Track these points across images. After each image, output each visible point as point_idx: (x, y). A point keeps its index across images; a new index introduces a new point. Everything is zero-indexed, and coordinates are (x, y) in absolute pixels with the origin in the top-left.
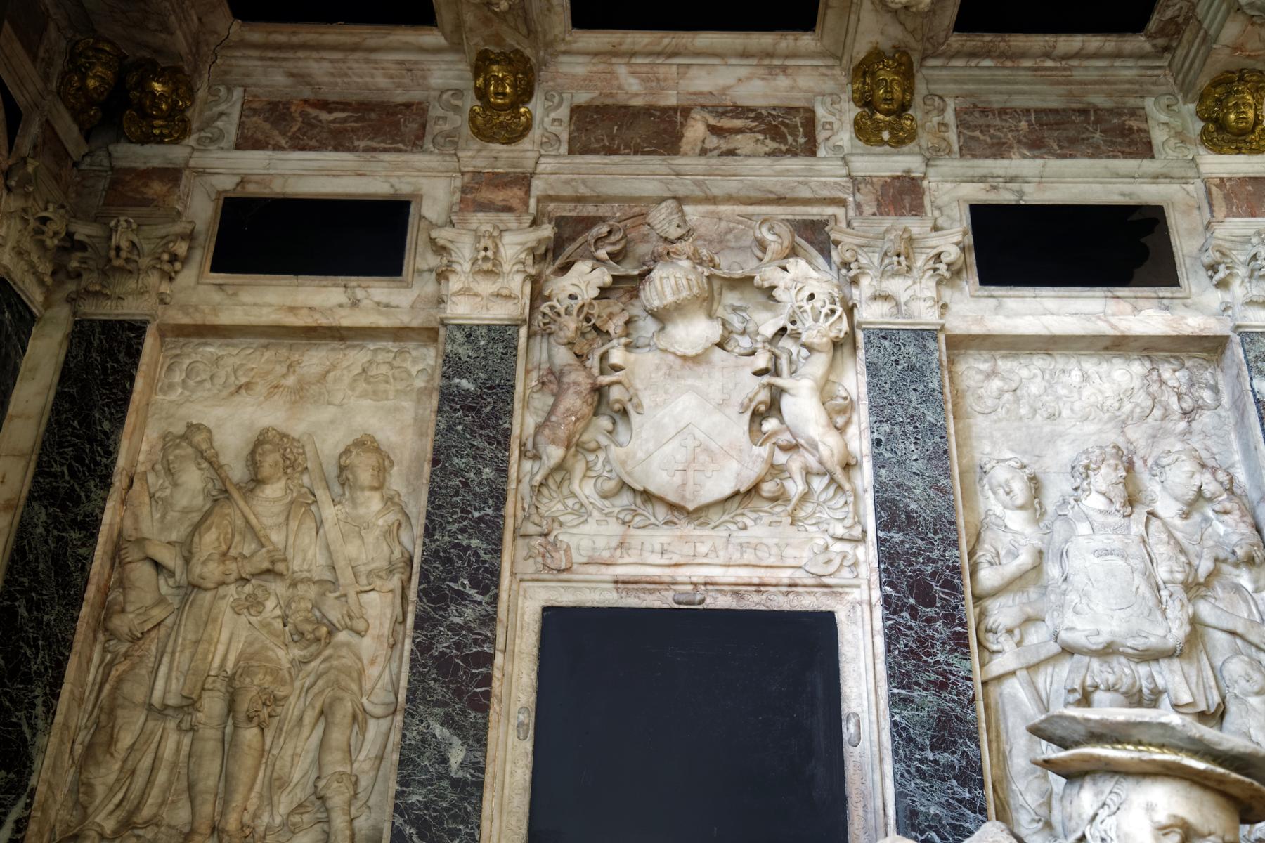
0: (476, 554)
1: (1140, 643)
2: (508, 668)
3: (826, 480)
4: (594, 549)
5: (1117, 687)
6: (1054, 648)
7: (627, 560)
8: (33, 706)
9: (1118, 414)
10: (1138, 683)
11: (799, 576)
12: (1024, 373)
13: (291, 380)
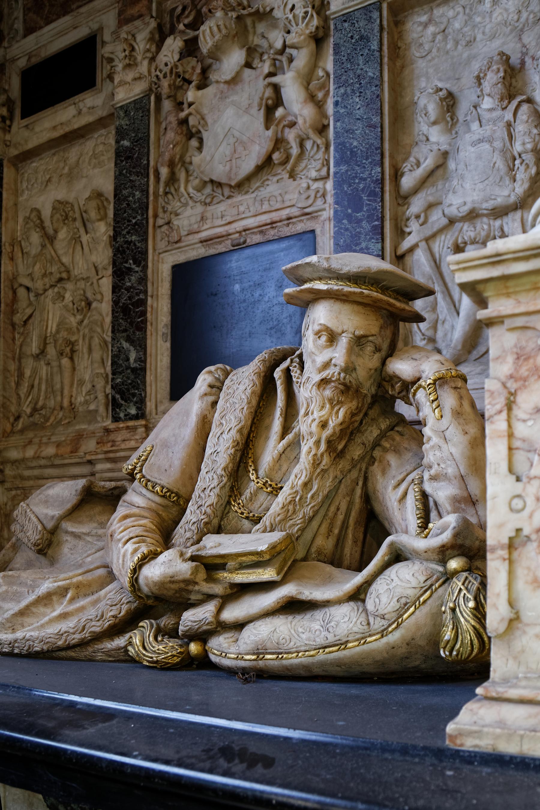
4: (190, 225)
7: (206, 227)
11: (294, 211)
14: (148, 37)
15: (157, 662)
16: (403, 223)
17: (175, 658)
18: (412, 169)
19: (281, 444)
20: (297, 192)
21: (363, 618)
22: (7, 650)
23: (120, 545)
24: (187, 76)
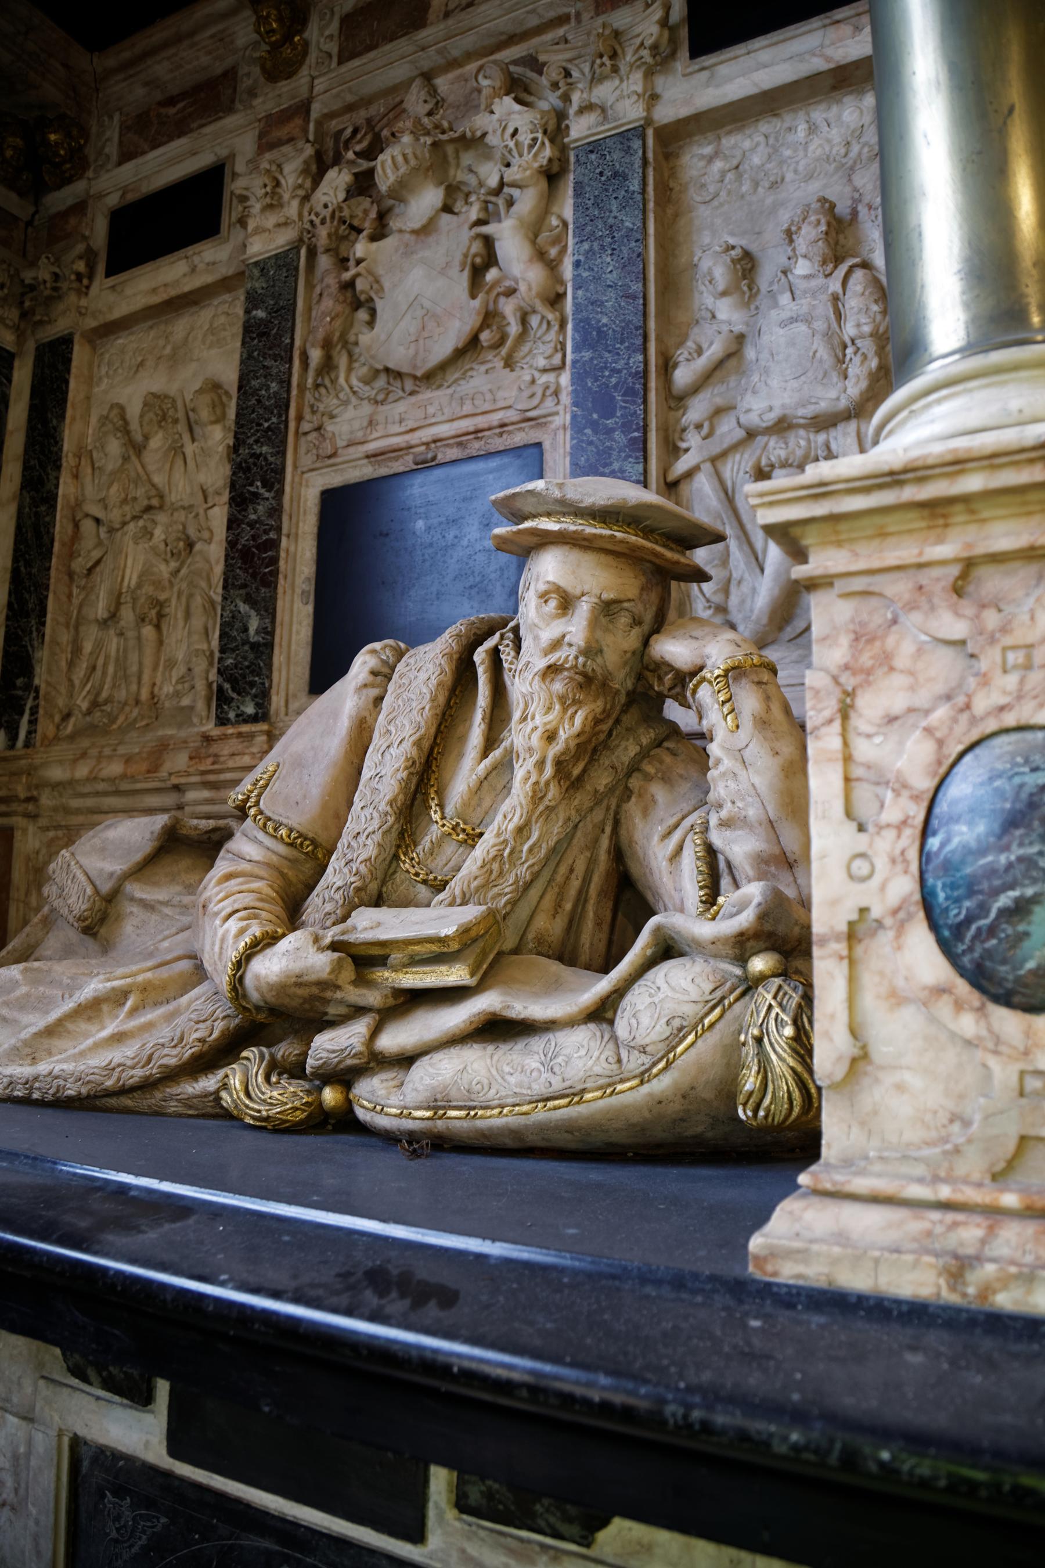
0: (266, 459)
1: (809, 411)
2: (292, 549)
3: (539, 317)
4: (352, 432)
6: (740, 434)
7: (375, 435)
8: (31, 632)
9: (844, 161)
11: (511, 415)
12: (747, 144)
13: (168, 351)
14: (301, 168)
15: (267, 1119)
16: (677, 436)
17: (298, 1112)
19: (482, 765)
20: (516, 387)
21: (609, 1052)
22: (20, 1094)
23: (218, 922)
24: (356, 223)
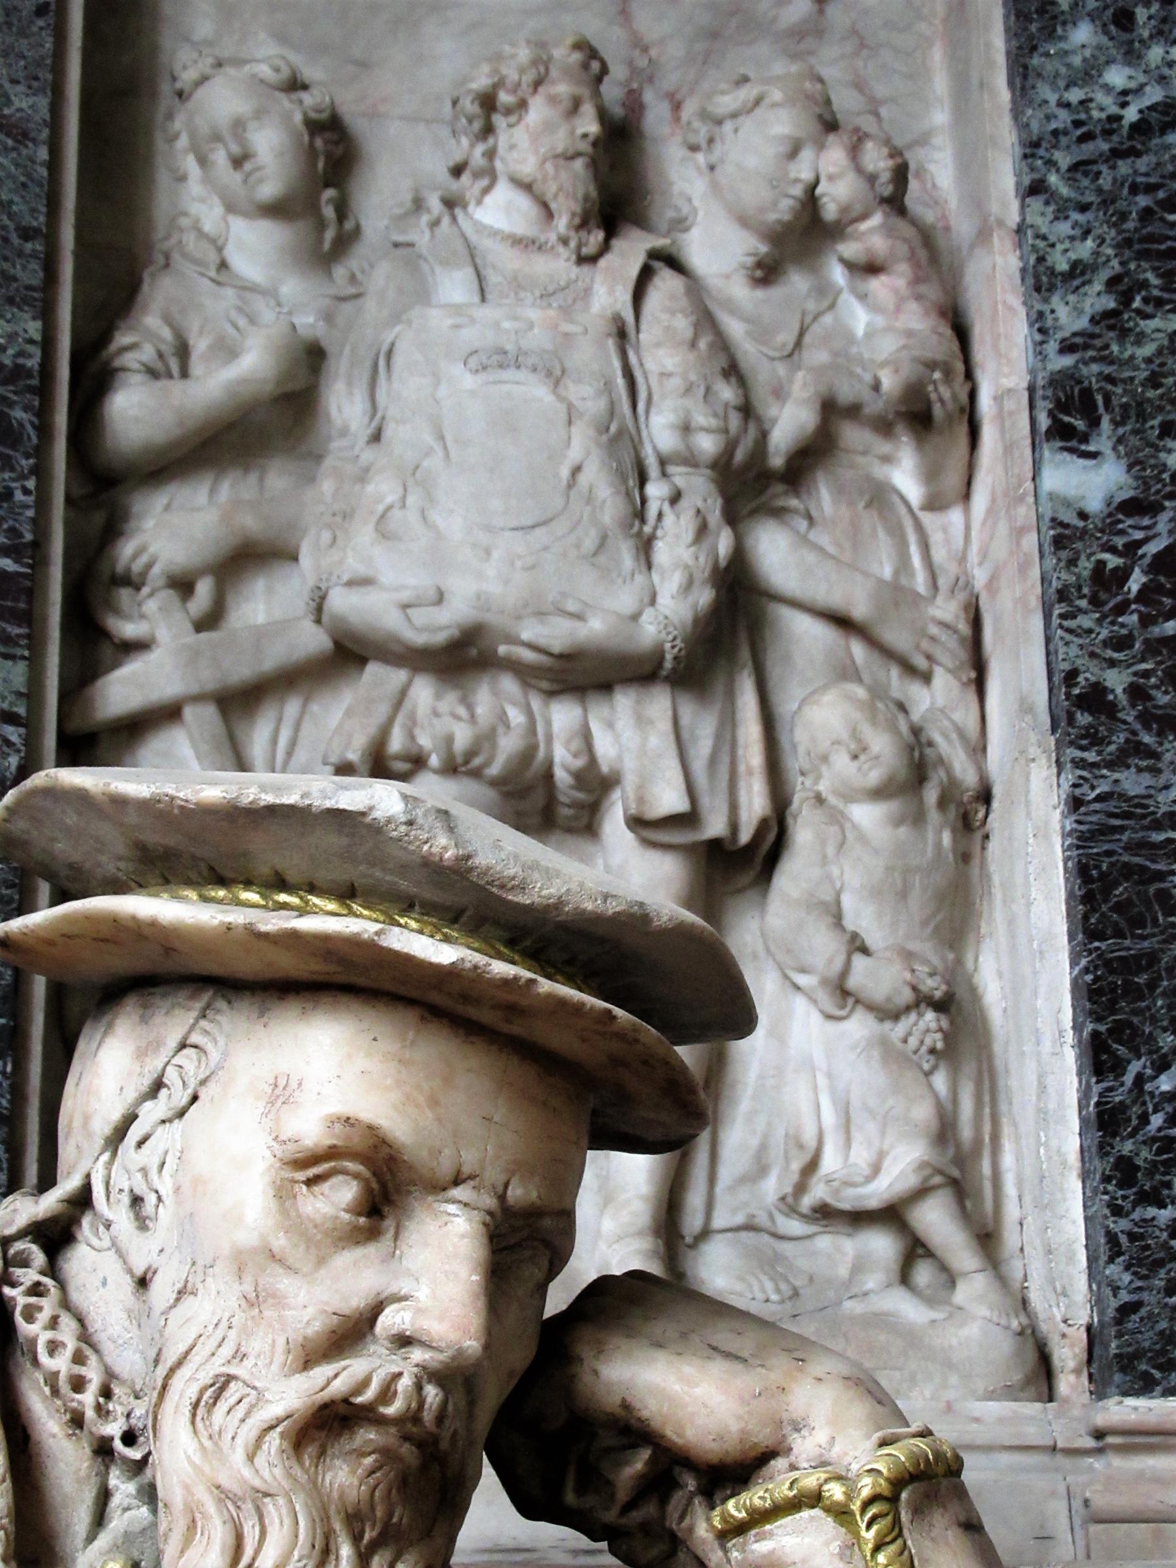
5: (477, 761)
10: (541, 754)
18: (158, 366)
